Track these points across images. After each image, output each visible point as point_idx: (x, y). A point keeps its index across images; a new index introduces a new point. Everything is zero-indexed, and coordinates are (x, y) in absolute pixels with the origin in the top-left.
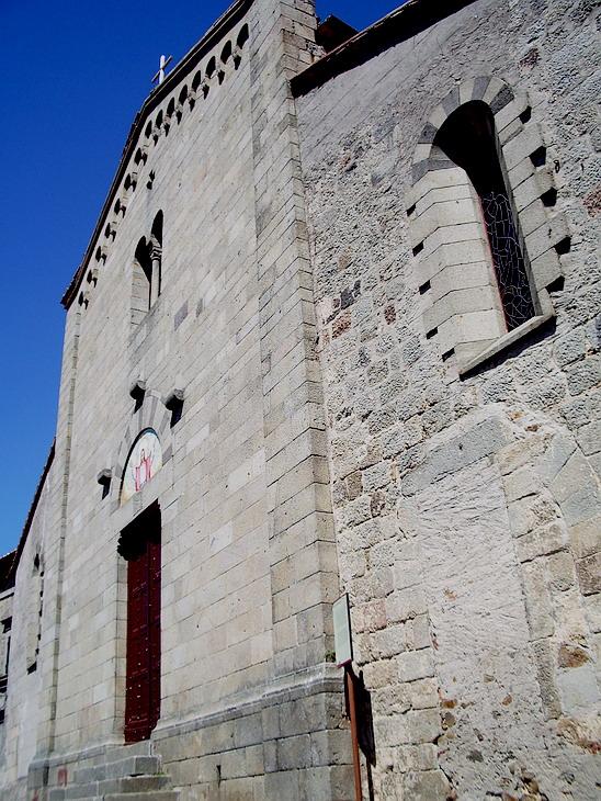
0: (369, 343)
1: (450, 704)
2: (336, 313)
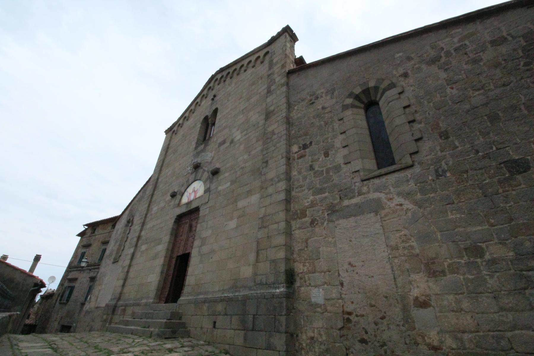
0: (314, 163)
1: (350, 313)
2: (299, 151)
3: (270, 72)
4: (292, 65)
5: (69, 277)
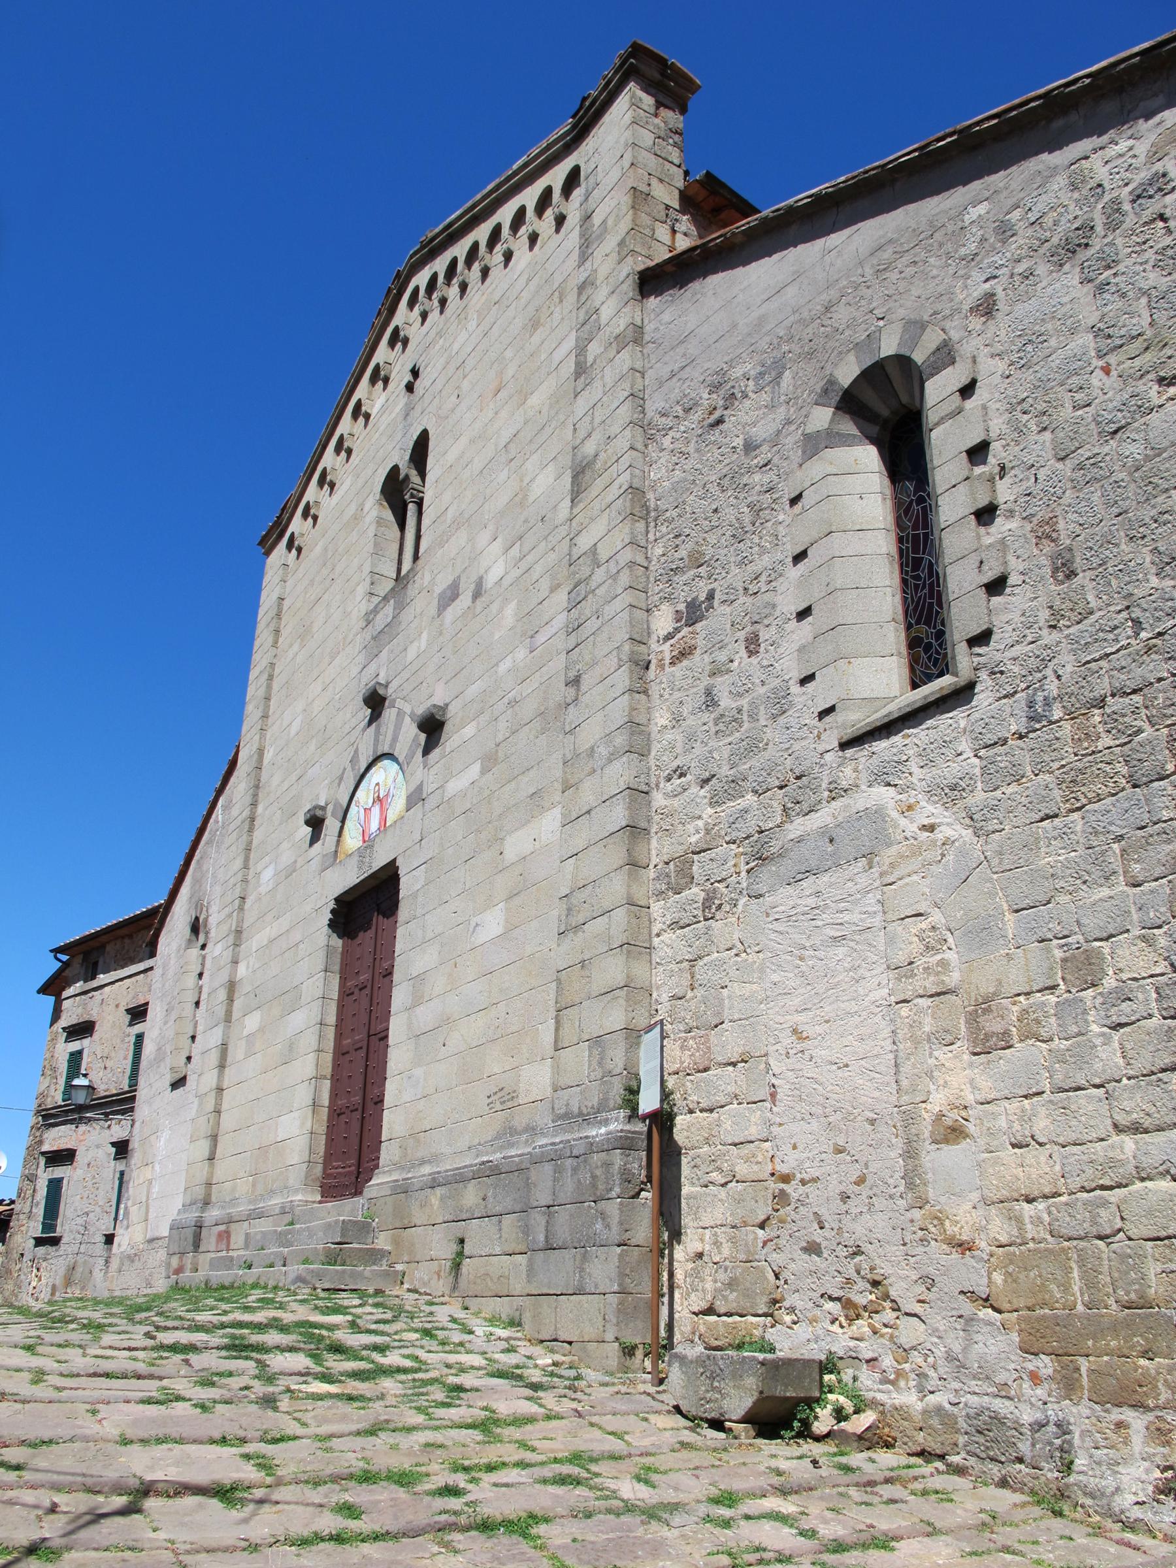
0: (719, 680)
1: (786, 1179)
2: (677, 630)
5: (46, 1148)
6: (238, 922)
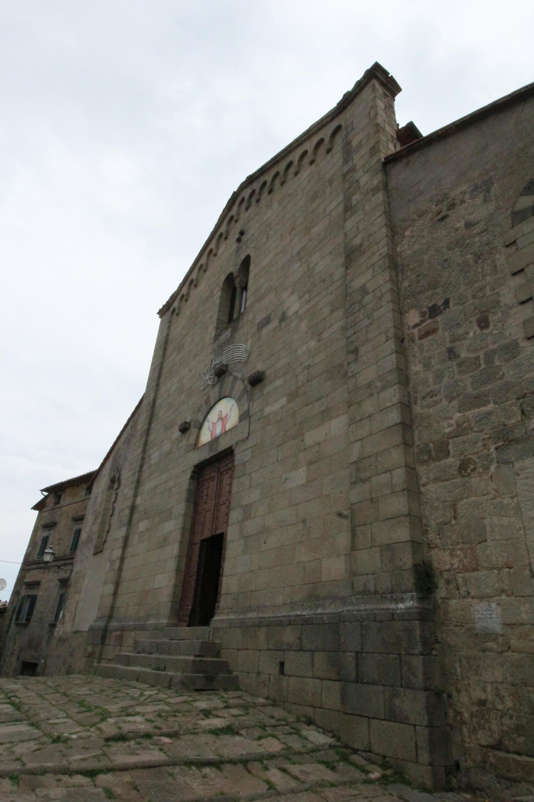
0: (458, 343)
2: (422, 322)
3: (346, 169)
4: (391, 146)
5: (26, 580)
6: (138, 477)
